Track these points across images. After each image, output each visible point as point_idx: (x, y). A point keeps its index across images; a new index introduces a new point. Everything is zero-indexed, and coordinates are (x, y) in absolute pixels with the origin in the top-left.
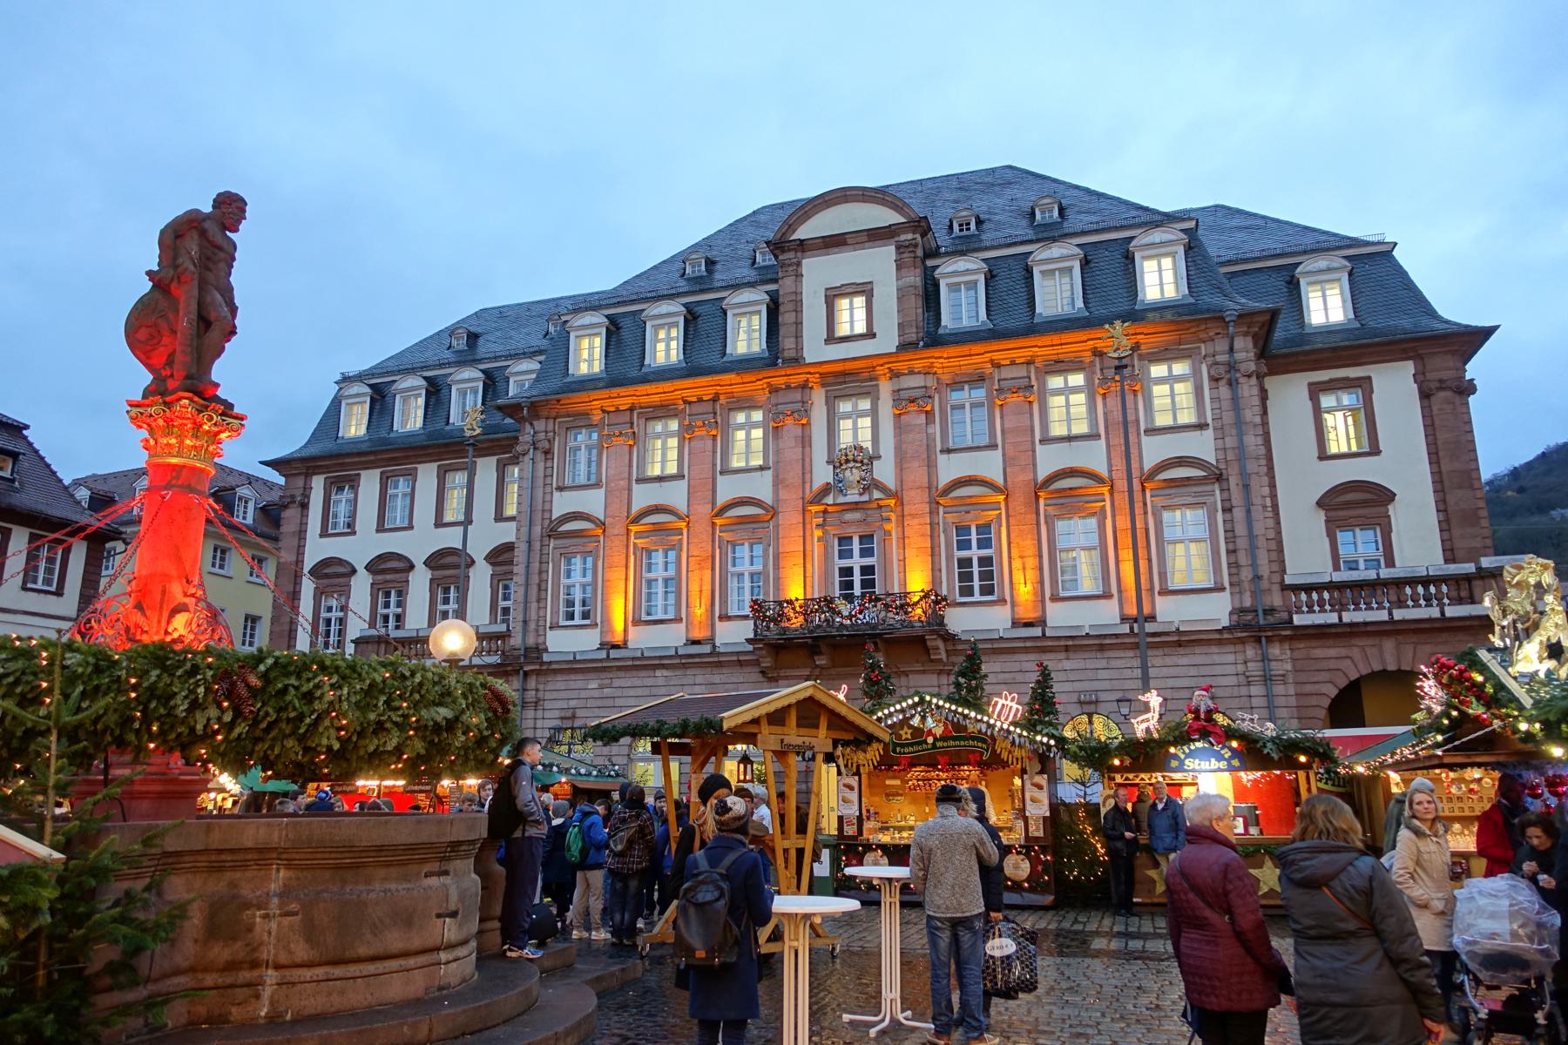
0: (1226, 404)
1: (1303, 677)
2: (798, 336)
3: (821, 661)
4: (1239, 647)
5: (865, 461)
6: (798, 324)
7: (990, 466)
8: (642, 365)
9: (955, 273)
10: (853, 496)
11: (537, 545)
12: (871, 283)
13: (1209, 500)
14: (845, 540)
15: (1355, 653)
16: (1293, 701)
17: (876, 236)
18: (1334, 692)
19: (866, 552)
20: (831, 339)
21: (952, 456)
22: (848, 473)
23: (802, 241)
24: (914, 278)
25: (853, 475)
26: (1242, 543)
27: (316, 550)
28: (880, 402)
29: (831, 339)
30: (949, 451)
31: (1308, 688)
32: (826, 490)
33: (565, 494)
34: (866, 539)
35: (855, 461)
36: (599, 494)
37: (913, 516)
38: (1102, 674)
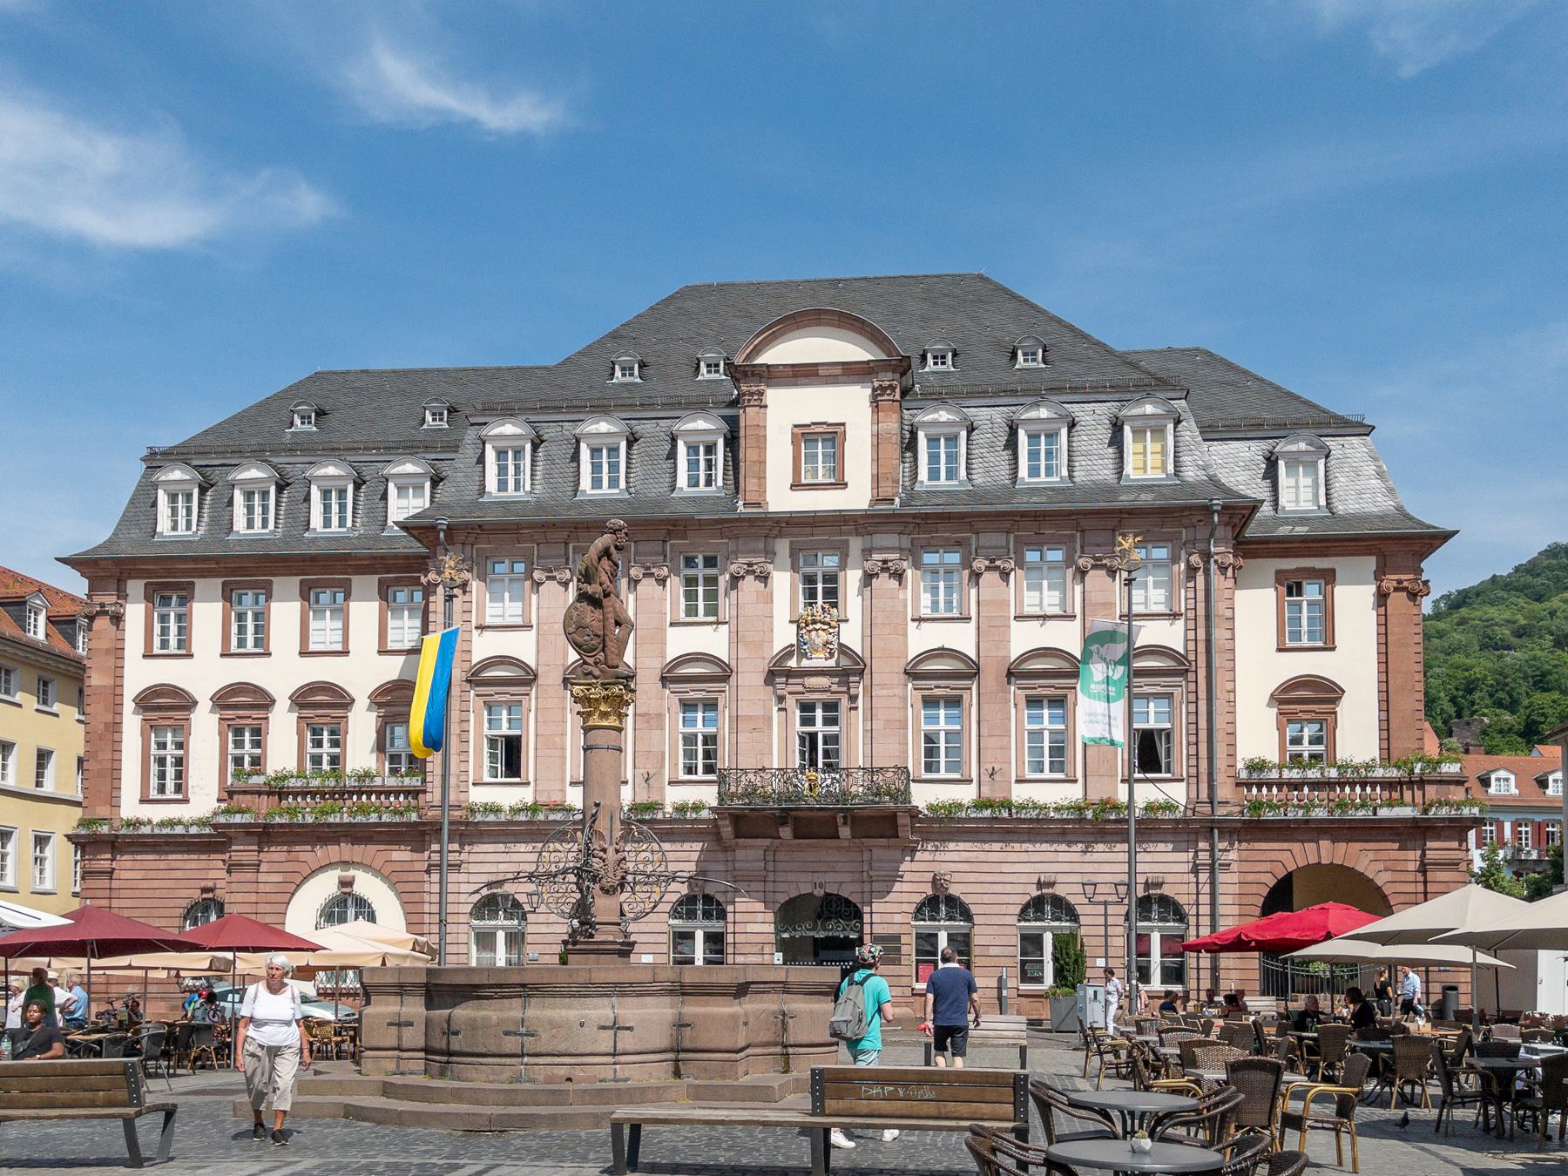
0: (1201, 595)
1: (1246, 867)
2: (762, 478)
3: (786, 832)
4: (1193, 837)
5: (833, 624)
6: (762, 463)
7: (962, 638)
8: (576, 491)
9: (935, 423)
10: (819, 661)
11: (455, 691)
12: (843, 424)
13: (1177, 691)
14: (807, 708)
15: (1296, 847)
16: (1235, 889)
17: (850, 372)
18: (1272, 882)
19: (829, 721)
20: (796, 486)
21: (924, 625)
22: (814, 633)
23: (768, 366)
24: (891, 425)
25: (819, 638)
26: (1203, 735)
27: (139, 674)
28: (849, 560)
29: (796, 486)
30: (920, 620)
31: (1250, 877)
32: (788, 653)
33: (487, 634)
34: (830, 707)
35: (824, 623)
36: (531, 635)
37: (883, 686)
38: (1062, 857)
